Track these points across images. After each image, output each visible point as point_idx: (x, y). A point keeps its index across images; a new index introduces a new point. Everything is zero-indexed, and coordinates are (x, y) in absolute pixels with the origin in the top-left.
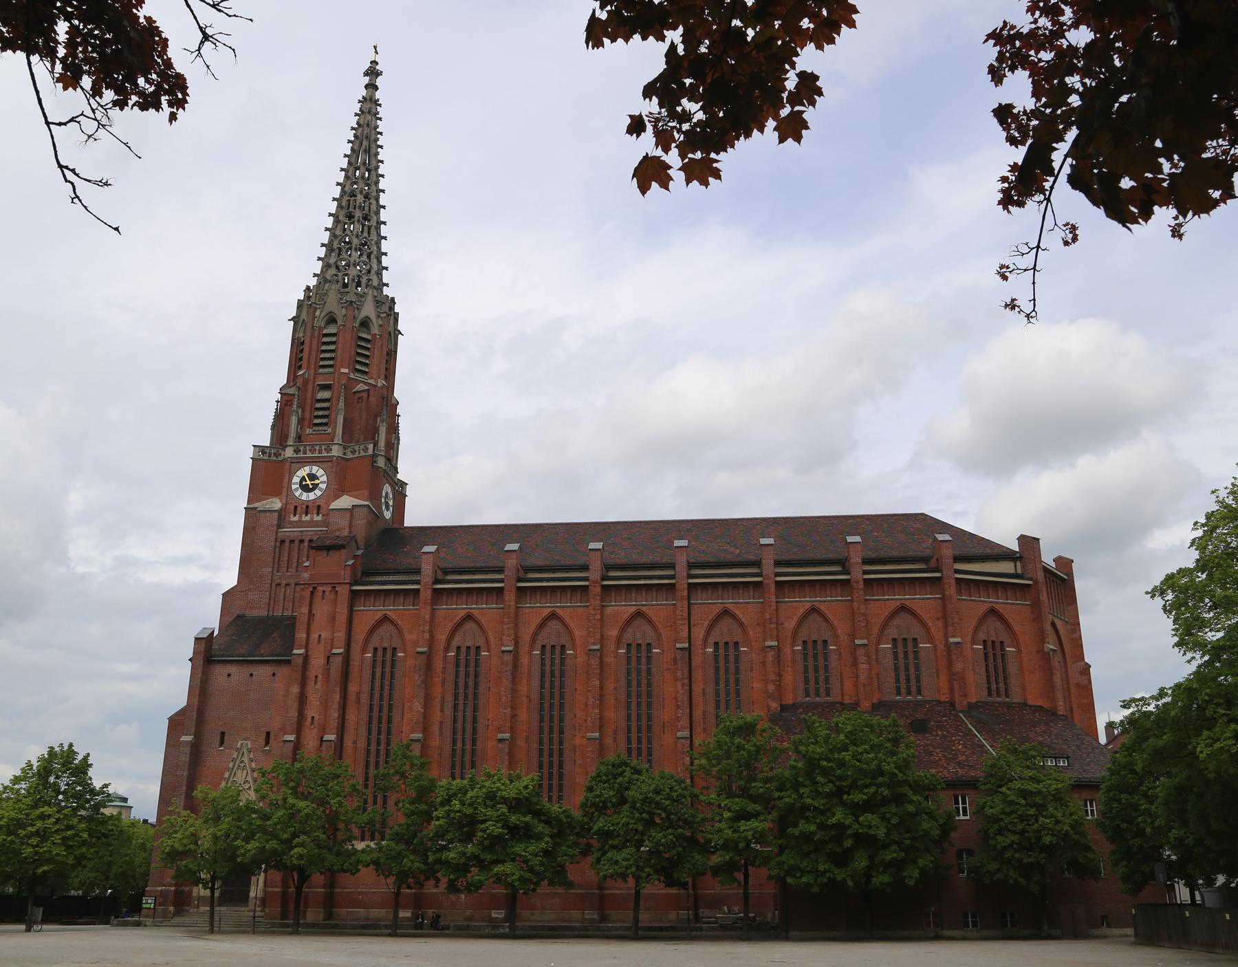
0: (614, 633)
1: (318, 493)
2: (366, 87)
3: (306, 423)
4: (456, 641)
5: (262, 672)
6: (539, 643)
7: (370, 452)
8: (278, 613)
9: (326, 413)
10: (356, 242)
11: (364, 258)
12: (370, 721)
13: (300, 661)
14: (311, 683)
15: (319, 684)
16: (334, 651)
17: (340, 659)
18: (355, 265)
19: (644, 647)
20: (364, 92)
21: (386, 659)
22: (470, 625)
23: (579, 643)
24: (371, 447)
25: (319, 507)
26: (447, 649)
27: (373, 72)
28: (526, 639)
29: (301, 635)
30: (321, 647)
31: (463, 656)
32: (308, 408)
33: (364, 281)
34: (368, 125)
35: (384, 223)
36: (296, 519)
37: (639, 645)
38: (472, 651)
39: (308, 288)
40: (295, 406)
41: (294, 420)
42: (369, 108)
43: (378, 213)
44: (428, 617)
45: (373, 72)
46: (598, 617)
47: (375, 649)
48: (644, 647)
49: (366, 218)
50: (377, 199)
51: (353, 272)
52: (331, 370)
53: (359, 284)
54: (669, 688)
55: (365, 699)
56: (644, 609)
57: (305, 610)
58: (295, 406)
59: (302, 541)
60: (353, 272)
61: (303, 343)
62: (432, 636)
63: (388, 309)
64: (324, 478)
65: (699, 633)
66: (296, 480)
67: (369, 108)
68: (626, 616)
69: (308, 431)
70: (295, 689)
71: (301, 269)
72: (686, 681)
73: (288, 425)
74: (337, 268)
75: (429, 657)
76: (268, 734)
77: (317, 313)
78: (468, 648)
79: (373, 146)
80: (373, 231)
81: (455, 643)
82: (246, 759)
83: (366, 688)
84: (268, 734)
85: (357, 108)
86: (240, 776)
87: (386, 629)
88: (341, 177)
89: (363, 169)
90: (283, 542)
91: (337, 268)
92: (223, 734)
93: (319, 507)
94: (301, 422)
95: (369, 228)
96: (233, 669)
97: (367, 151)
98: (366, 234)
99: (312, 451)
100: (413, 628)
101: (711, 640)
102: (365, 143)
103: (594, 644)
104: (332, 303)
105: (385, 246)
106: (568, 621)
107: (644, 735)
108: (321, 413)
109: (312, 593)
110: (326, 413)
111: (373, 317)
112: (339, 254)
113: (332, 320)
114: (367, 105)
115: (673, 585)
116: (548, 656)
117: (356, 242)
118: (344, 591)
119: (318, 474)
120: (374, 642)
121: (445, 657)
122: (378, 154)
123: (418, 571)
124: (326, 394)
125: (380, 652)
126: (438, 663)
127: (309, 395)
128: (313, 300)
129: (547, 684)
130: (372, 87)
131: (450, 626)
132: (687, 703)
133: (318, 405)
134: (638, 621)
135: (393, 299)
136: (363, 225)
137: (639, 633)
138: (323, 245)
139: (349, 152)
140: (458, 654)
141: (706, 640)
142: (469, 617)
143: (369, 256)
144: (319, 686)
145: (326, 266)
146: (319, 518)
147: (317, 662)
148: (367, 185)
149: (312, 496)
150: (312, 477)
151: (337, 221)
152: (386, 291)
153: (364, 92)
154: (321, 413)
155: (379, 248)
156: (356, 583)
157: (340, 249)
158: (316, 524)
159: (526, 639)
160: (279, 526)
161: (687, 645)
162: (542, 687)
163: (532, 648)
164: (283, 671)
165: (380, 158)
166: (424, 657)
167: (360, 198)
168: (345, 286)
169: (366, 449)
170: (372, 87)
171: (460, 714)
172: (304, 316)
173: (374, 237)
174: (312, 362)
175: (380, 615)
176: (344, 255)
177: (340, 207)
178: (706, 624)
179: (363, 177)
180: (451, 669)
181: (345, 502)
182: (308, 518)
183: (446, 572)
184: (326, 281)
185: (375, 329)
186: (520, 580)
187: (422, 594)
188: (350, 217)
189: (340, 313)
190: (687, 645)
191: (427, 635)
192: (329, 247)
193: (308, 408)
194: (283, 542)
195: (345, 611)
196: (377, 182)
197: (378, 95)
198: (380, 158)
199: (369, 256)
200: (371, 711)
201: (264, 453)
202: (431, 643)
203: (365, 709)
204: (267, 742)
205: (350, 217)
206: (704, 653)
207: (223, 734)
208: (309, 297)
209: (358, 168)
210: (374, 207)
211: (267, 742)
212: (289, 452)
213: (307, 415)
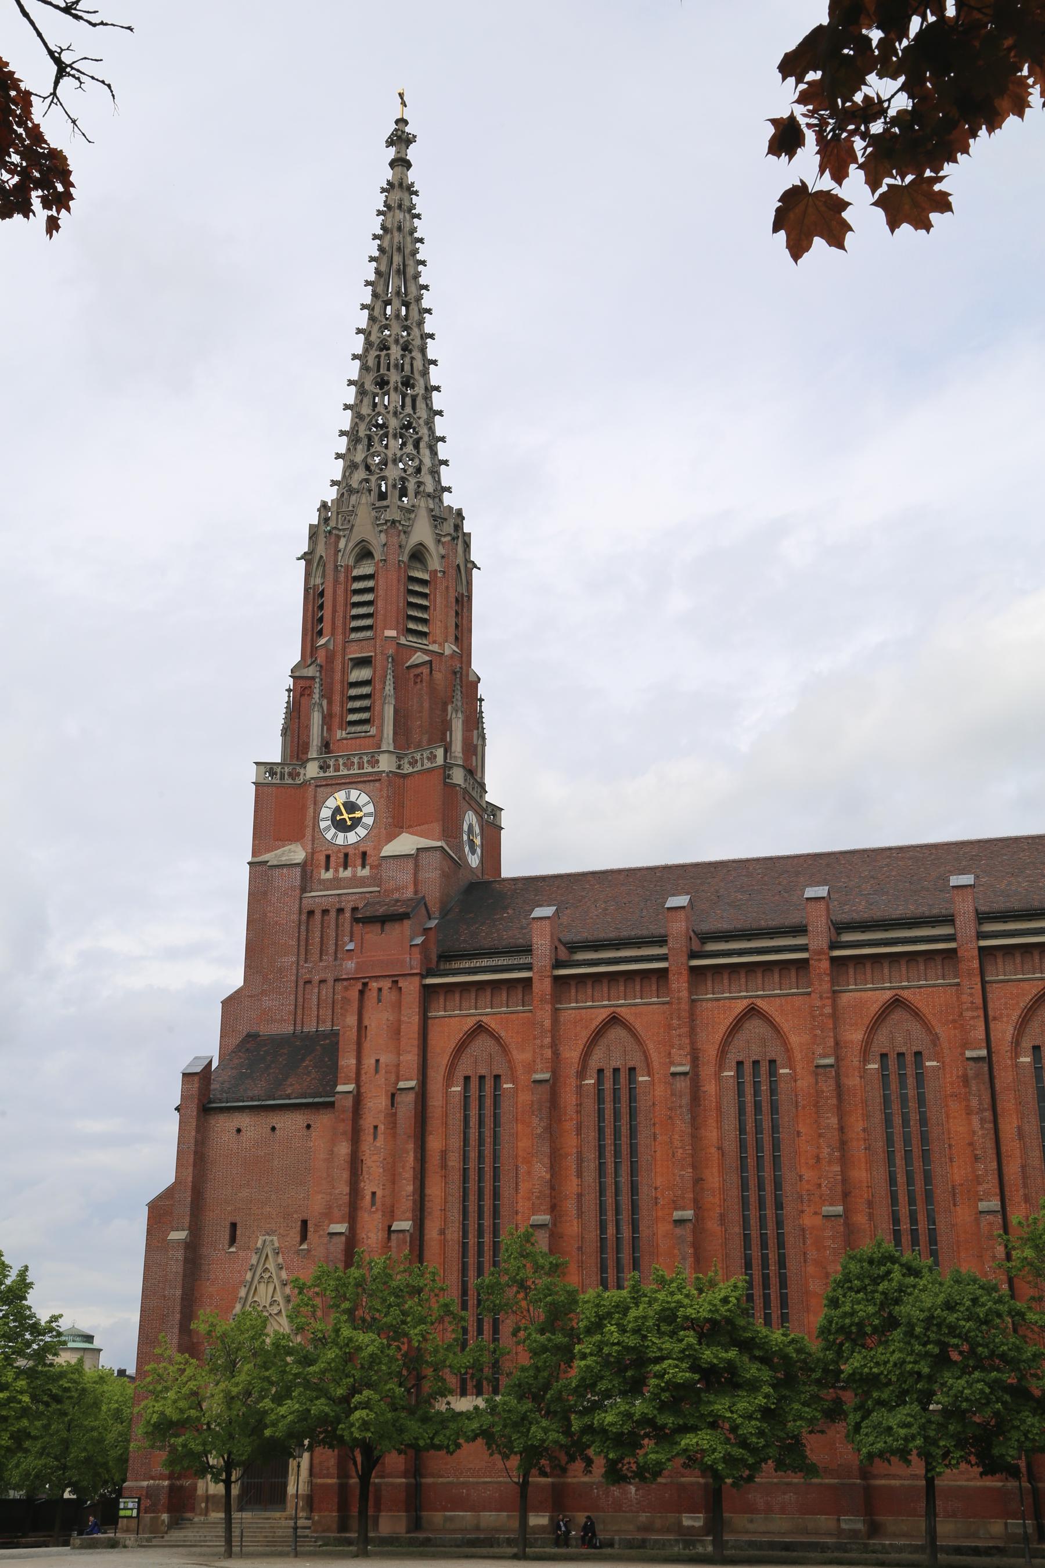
0: (855, 1036)
1: (361, 831)
2: (393, 164)
3: (336, 721)
4: (597, 1059)
5: (290, 1123)
6: (732, 1057)
7: (440, 760)
8: (310, 1027)
9: (366, 703)
10: (394, 423)
11: (410, 448)
12: (465, 1197)
13: (349, 1102)
14: (367, 1138)
15: (381, 1138)
16: (402, 1085)
17: (410, 1097)
18: (395, 462)
19: (909, 1059)
20: (388, 174)
21: (485, 1095)
22: (617, 1033)
23: (798, 1056)
24: (440, 753)
25: (364, 854)
26: (581, 1074)
27: (401, 139)
28: (710, 1052)
29: (347, 1061)
30: (381, 1079)
31: (608, 1085)
32: (337, 698)
33: (411, 486)
34: (399, 229)
36: (329, 875)
37: (901, 1055)
38: (623, 1077)
39: (324, 506)
40: (316, 696)
41: (316, 718)
43: (425, 373)
44: (547, 1023)
45: (401, 139)
46: (828, 1010)
47: (467, 1079)
48: (909, 1059)
49: (407, 383)
50: (423, 350)
51: (393, 472)
53: (403, 493)
54: (959, 1126)
55: (454, 1161)
56: (905, 994)
57: (352, 1020)
58: (316, 696)
59: (340, 911)
61: (322, 594)
62: (556, 1054)
63: (452, 528)
64: (370, 808)
65: (1004, 1031)
66: (326, 813)
68: (875, 1008)
69: (340, 734)
70: (344, 1149)
72: (988, 1114)
73: (308, 727)
74: (368, 468)
75: (553, 1088)
76: (304, 1223)
77: (342, 544)
78: (616, 1070)
79: (410, 262)
80: (420, 404)
81: (594, 1063)
82: (271, 1265)
83: (455, 1142)
84: (304, 1223)
85: (379, 201)
86: (264, 1295)
87: (482, 1045)
88: (362, 319)
89: (396, 302)
90: (311, 913)
91: (368, 468)
92: (234, 1226)
93: (364, 854)
94: (327, 719)
95: (414, 399)
96: (244, 1120)
97: (402, 272)
98: (408, 410)
99: (349, 765)
100: (523, 1040)
101: (1027, 1044)
102: (397, 259)
103: (824, 1056)
104: (364, 526)
105: (440, 426)
106: (778, 1019)
107: (920, 1207)
108: (358, 704)
109: (362, 992)
110: (366, 703)
112: (370, 446)
113: (365, 553)
114: (396, 195)
115: (954, 951)
116: (748, 1078)
117: (394, 423)
118: (411, 988)
119: (360, 802)
120: (465, 1068)
121: (580, 1087)
123: (528, 950)
124: (364, 674)
125: (474, 1084)
126: (569, 1098)
127: (338, 676)
128: (333, 523)
129: (750, 1126)
130: (401, 163)
131: (585, 1035)
132: (991, 1152)
133: (353, 692)
134: (898, 1015)
135: (459, 513)
136: (404, 396)
137: (901, 1036)
138: (342, 433)
139: (372, 277)
140: (600, 1081)
141: (1017, 1042)
142: (614, 1020)
144: (380, 1142)
145: (351, 467)
146: (366, 872)
147: (376, 1104)
148: (406, 328)
149: (352, 837)
150: (351, 807)
151: (362, 392)
152: (448, 499)
153: (388, 174)
154: (358, 704)
156: (430, 973)
157: (370, 438)
158: (362, 882)
159: (710, 1052)
160: (303, 890)
161: (984, 1053)
162: (742, 1130)
163: (721, 1066)
164: (323, 1121)
165: (422, 281)
166: (547, 1086)
167: (395, 351)
168: (382, 496)
169: (433, 758)
170: (401, 163)
171: (609, 1180)
172: (321, 550)
173: (422, 412)
174: (339, 623)
175: (470, 1022)
176: (377, 447)
177: (365, 368)
178: (1015, 1015)
179: (398, 316)
180: (590, 1104)
181: (405, 844)
182: (348, 873)
183: (574, 947)
184: (351, 491)
185: (435, 563)
186: (693, 955)
187: (536, 986)
188: (382, 383)
189: (377, 542)
190: (984, 1053)
191: (548, 1053)
192: (352, 435)
193: (337, 698)
194: (311, 913)
195: (416, 1019)
196: (421, 323)
197: (412, 176)
198: (422, 281)
200: (465, 1178)
201: (272, 773)
202: (556, 1064)
203: (456, 1177)
204: (304, 1238)
205: (382, 383)
206: (1016, 1065)
207: (234, 1226)
208: (327, 520)
209: (388, 302)
210: (418, 364)
211: (304, 1238)
212: (312, 770)
213: (337, 709)
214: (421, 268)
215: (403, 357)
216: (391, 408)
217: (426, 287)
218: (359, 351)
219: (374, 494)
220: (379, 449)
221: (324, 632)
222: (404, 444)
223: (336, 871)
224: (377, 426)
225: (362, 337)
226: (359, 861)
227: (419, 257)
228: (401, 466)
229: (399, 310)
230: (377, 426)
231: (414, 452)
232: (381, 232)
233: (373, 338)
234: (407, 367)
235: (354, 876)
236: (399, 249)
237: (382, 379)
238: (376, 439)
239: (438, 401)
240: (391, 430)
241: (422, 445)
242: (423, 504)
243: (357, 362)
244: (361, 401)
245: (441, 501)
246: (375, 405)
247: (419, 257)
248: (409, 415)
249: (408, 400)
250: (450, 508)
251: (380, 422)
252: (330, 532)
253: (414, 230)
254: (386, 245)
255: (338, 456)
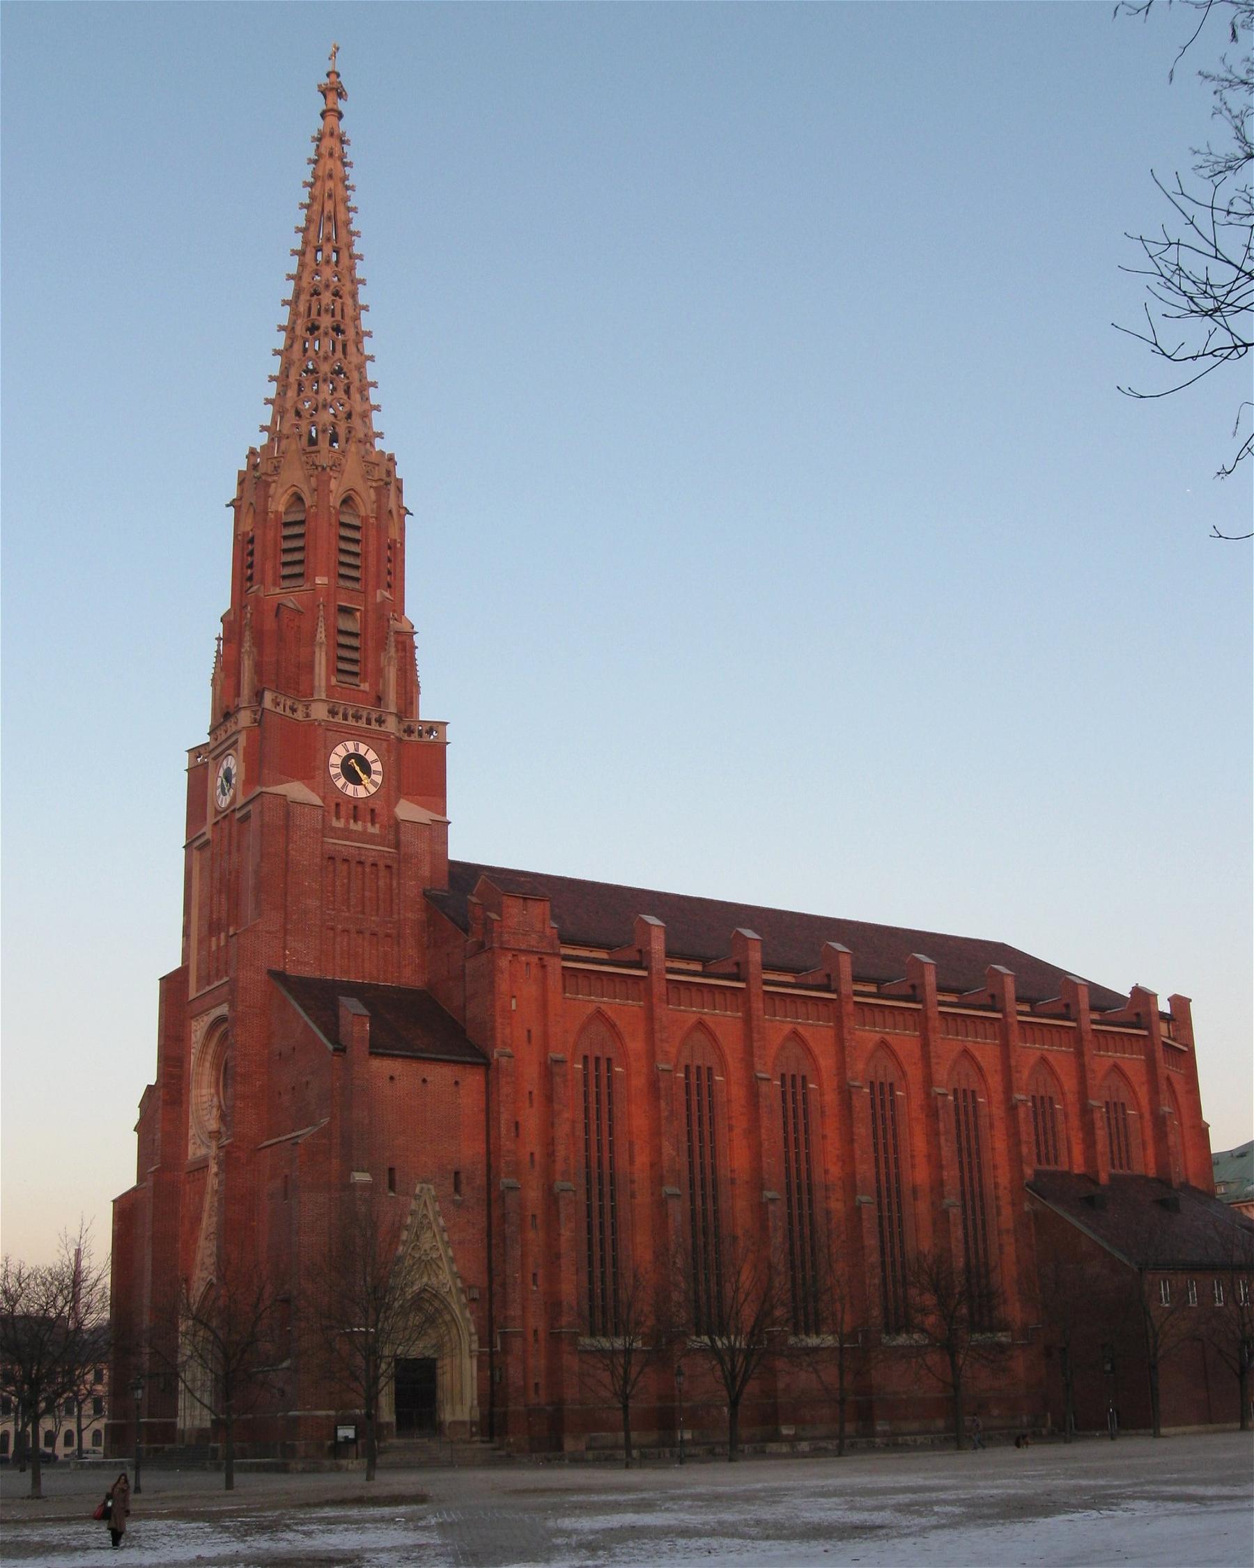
10: (325, 368)
11: (340, 394)
18: (325, 406)
20: (320, 124)
27: (333, 90)
34: (330, 176)
35: (369, 334)
36: (339, 824)
39: (253, 452)
42: (330, 151)
45: (333, 90)
50: (354, 295)
51: (326, 416)
52: (357, 586)
53: (334, 438)
60: (326, 416)
61: (252, 541)
63: (384, 478)
67: (330, 151)
71: (236, 417)
74: (298, 414)
76: (457, 1173)
79: (341, 208)
80: (351, 349)
84: (457, 1173)
86: (427, 1240)
88: (293, 265)
89: (328, 248)
91: (298, 414)
95: (344, 346)
97: (333, 218)
98: (339, 354)
99: (357, 717)
105: (372, 371)
111: (360, 486)
112: (300, 391)
114: (328, 142)
117: (325, 368)
122: (349, 222)
128: (262, 469)
135: (391, 458)
138: (272, 379)
139: (303, 224)
143: (347, 392)
145: (280, 412)
146: (374, 830)
151: (292, 339)
152: (379, 445)
153: (320, 124)
155: (362, 377)
158: (371, 839)
165: (353, 227)
167: (327, 297)
168: (313, 442)
173: (354, 359)
176: (307, 392)
177: (295, 314)
179: (328, 262)
182: (352, 826)
188: (313, 329)
192: (282, 380)
196: (352, 269)
197: (343, 126)
198: (353, 227)
199: (347, 392)
204: (457, 1189)
205: (313, 329)
208: (255, 467)
209: (319, 249)
210: (349, 311)
214: (352, 214)
215: (333, 302)
216: (321, 354)
217: (357, 234)
218: (289, 297)
219: (305, 440)
220: (311, 394)
221: (256, 577)
222: (334, 389)
223: (347, 822)
224: (307, 371)
225: (292, 283)
226: (369, 817)
227: (349, 204)
228: (332, 411)
229: (329, 256)
230: (307, 371)
231: (345, 397)
232: (312, 180)
233: (304, 284)
234: (338, 312)
235: (365, 831)
236: (330, 196)
237: (338, 326)
238: (307, 384)
239: (368, 346)
240: (321, 375)
241: (353, 390)
242: (353, 449)
243: (287, 308)
244: (291, 346)
245: (372, 445)
246: (305, 350)
247: (349, 204)
248: (339, 360)
249: (339, 348)
250: (382, 453)
251: (311, 367)
252: (259, 478)
253: (346, 178)
254: (317, 192)
255: (268, 401)
